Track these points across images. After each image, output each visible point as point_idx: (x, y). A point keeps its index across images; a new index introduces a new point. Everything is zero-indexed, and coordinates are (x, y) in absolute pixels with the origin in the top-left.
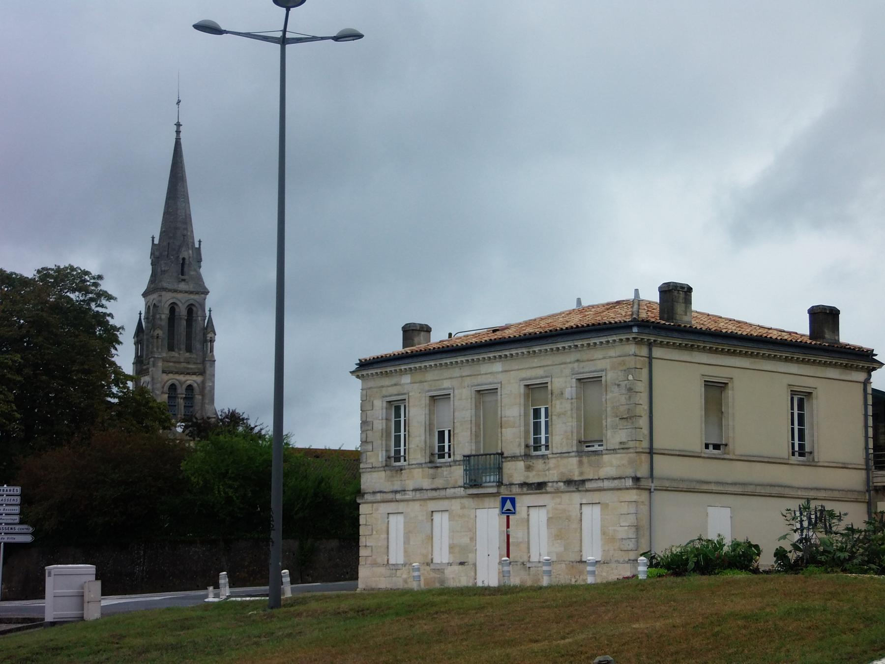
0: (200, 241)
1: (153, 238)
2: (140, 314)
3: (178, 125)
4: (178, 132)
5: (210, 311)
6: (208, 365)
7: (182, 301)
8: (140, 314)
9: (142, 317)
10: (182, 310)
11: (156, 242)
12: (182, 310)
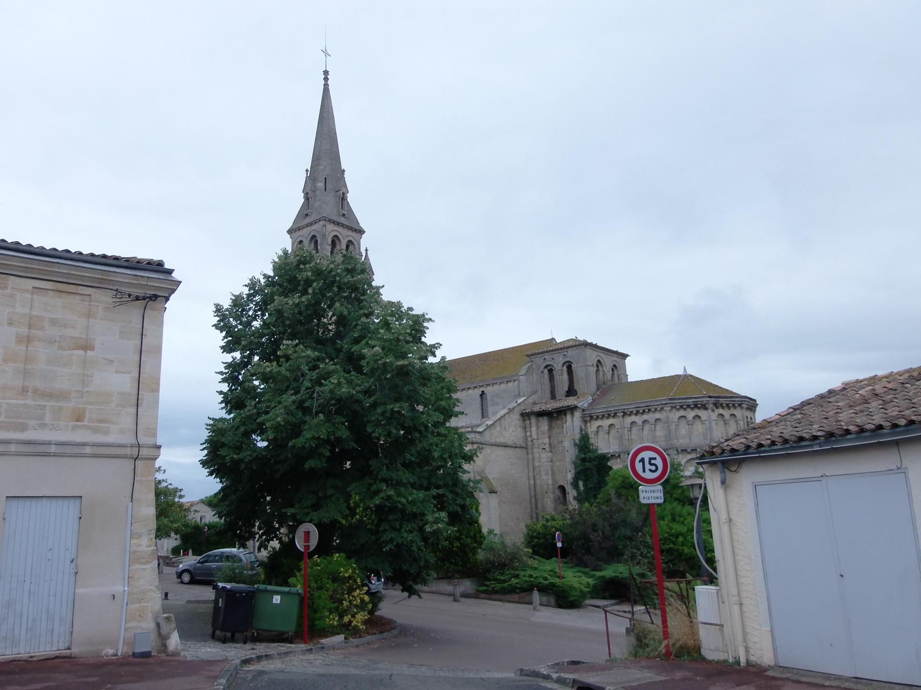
3: (326, 73)
4: (326, 79)
5: (366, 250)
12: (344, 243)
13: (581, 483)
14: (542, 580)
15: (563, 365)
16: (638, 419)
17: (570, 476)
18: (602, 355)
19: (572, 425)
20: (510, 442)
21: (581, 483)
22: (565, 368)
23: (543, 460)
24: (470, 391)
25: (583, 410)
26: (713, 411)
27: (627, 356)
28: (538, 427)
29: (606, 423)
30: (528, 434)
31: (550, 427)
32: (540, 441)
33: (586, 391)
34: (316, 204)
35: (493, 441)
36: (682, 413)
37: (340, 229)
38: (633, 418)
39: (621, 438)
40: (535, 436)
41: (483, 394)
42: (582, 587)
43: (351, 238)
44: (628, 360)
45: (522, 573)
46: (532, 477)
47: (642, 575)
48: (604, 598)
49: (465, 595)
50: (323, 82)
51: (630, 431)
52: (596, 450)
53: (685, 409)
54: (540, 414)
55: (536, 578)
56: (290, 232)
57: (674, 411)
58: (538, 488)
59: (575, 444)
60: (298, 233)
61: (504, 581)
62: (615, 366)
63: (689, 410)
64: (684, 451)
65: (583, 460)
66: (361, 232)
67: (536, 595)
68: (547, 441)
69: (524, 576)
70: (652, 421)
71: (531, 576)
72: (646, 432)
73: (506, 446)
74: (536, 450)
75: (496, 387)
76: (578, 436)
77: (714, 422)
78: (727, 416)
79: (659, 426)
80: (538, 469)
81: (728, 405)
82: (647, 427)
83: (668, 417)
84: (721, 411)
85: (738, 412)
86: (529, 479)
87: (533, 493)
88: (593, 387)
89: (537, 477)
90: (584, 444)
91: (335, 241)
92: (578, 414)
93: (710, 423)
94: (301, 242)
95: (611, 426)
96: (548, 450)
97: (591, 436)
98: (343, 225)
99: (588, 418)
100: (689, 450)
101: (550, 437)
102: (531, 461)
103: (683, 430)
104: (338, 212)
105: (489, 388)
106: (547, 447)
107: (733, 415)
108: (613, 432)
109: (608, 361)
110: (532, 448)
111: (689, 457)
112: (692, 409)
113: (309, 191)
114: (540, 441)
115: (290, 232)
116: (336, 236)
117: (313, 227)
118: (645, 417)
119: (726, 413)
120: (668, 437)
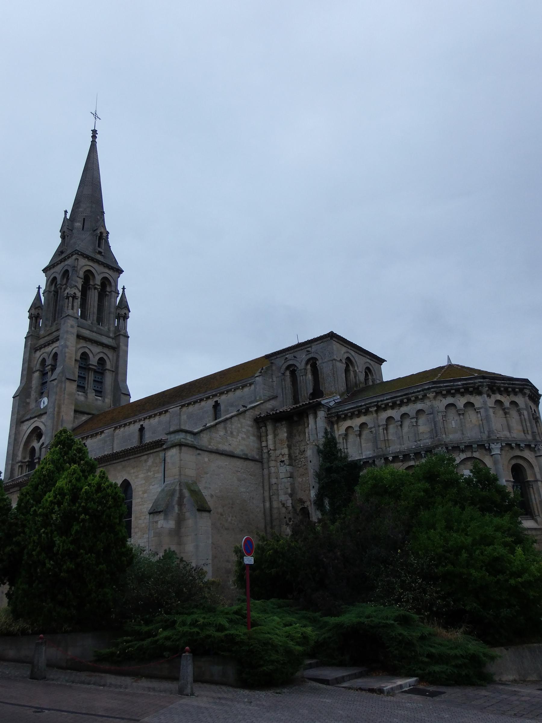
2: (39, 288)
3: (94, 132)
4: (94, 137)
5: (124, 288)
6: (122, 338)
8: (39, 288)
9: (42, 291)
12: (98, 281)
13: (326, 501)
14: (211, 631)
15: (307, 364)
16: (395, 413)
17: (313, 494)
18: (353, 353)
19: (316, 426)
20: (237, 452)
21: (326, 501)
22: (309, 367)
23: (282, 476)
24: (203, 403)
25: (329, 409)
26: (489, 396)
27: (384, 361)
28: (275, 435)
29: (356, 422)
30: (264, 444)
31: (290, 436)
32: (278, 452)
33: (333, 389)
34: (72, 241)
35: (213, 446)
36: (450, 400)
37: (95, 265)
38: (390, 413)
39: (375, 441)
40: (271, 446)
41: (216, 406)
42: (291, 644)
43: (107, 275)
44: (384, 366)
45: (179, 619)
46: (267, 499)
47: (404, 621)
48: (341, 664)
49: (75, 666)
50: (91, 139)
51: (387, 429)
52: (346, 457)
53: (453, 395)
54: (277, 418)
55: (203, 627)
56: (45, 270)
57: (440, 397)
58: (275, 511)
59: (319, 451)
60: (52, 271)
61: (149, 634)
62: (368, 368)
63: (458, 396)
64: (456, 448)
65: (329, 470)
66: (120, 271)
67: (187, 666)
68: (286, 451)
69: (184, 624)
70: (413, 413)
71: (194, 624)
72: (406, 429)
73: (231, 455)
74: (272, 464)
75: (231, 394)
76: (322, 441)
78: (507, 404)
79: (422, 420)
80: (274, 487)
81: (506, 389)
82: (407, 423)
83: (432, 407)
84: (499, 397)
85: (521, 400)
86: (264, 502)
87: (268, 518)
88: (342, 387)
89: (275, 497)
90: (329, 450)
91: (88, 276)
92: (321, 414)
93: (486, 410)
94: (55, 279)
95: (363, 425)
96: (287, 462)
97: (340, 440)
99: (335, 417)
100: (462, 447)
101: (289, 447)
102: (266, 477)
103: (453, 422)
104: (94, 249)
105: (223, 397)
106: (286, 458)
107: (513, 403)
108: (365, 432)
109: (360, 362)
110: (269, 461)
111: (463, 456)
112: (462, 394)
113: (66, 230)
114: (278, 452)
115: (45, 270)
116: (89, 271)
117: (66, 263)
118: (404, 409)
119: (506, 400)
120: (434, 432)
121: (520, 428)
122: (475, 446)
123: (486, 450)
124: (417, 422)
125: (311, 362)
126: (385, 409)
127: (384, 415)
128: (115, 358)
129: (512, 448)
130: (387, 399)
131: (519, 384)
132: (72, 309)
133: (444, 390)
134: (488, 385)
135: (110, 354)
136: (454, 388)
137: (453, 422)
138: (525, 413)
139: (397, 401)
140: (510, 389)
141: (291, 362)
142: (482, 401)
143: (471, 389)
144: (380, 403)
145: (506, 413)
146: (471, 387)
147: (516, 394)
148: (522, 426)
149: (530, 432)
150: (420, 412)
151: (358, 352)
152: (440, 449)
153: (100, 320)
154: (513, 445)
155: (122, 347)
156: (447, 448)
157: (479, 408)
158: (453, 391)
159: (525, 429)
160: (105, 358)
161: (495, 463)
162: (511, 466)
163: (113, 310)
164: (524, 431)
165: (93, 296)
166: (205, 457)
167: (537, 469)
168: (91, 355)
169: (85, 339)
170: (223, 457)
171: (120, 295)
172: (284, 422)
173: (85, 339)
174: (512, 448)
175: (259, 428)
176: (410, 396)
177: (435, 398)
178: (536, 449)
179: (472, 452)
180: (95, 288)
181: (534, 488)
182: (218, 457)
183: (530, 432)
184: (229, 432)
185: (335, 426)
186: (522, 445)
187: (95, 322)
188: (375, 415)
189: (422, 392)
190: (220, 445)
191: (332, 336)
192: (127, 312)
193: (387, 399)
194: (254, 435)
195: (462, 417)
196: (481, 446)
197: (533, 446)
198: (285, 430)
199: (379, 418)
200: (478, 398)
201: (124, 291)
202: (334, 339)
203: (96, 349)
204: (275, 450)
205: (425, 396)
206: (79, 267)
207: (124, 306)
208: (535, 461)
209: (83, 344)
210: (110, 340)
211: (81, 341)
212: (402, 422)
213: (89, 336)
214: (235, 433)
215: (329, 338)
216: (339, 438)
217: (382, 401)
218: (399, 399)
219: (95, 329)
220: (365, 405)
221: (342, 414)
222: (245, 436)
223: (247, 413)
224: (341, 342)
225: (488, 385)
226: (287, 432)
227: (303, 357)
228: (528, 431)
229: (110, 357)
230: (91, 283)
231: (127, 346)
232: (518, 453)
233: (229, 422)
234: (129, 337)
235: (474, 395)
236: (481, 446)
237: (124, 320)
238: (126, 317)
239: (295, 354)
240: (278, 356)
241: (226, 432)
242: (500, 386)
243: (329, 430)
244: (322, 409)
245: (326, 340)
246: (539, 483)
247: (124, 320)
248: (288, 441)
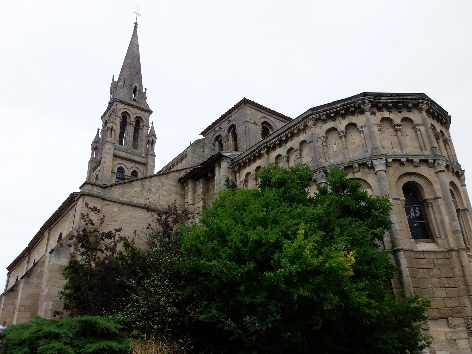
0: (146, 89)
1: (113, 76)
2: (98, 130)
3: (136, 24)
4: (136, 27)
5: (153, 123)
6: (150, 157)
7: (133, 113)
8: (98, 130)
9: (100, 131)
10: (132, 118)
11: (116, 79)
12: (132, 118)
15: (229, 132)
18: (272, 119)
22: (231, 134)
28: (194, 192)
30: (186, 201)
35: (125, 199)
43: (139, 115)
53: (334, 119)
57: (320, 124)
63: (339, 119)
66: (150, 112)
70: (296, 146)
77: (376, 129)
79: (306, 151)
84: (386, 114)
91: (125, 116)
93: (369, 128)
98: (132, 106)
101: (204, 200)
103: (335, 144)
107: (405, 120)
112: (343, 116)
114: (196, 206)
118: (290, 144)
119: (396, 117)
121: (417, 145)
122: (356, 165)
123: (369, 168)
124: (301, 154)
125: (232, 129)
126: (274, 148)
127: (273, 155)
128: (145, 171)
129: (402, 164)
130: (274, 138)
131: (411, 99)
132: (111, 137)
133: (322, 115)
134: (371, 102)
135: (141, 168)
136: (334, 110)
137: (335, 147)
138: (423, 129)
139: (282, 137)
140: (400, 105)
141: (218, 134)
142: (365, 119)
143: (352, 109)
144: (269, 144)
145: (396, 131)
146: (352, 107)
147: (409, 110)
148: (419, 142)
149: (428, 148)
150: (303, 143)
151: (279, 118)
152: (318, 173)
153: (135, 146)
154: (404, 160)
155: (150, 162)
156: (325, 172)
157: (362, 127)
158: (332, 115)
159: (423, 145)
160: (137, 171)
161: (379, 180)
162: (401, 185)
163: (144, 138)
164: (421, 147)
165: (130, 130)
166: (116, 208)
167: (437, 186)
168: (125, 169)
169: (120, 158)
170: (137, 209)
171: (150, 128)
172: (201, 180)
173: (120, 158)
174: (402, 164)
175: (183, 188)
176: (293, 128)
177: (314, 125)
178: (436, 164)
179: (354, 173)
180: (131, 124)
181: (435, 207)
182: (132, 209)
183: (428, 148)
184: (147, 189)
185: (237, 175)
186: (415, 160)
187: (131, 147)
188: (266, 156)
189: (302, 123)
190: (134, 199)
191: (245, 102)
192: (154, 139)
193: (274, 138)
194: (177, 193)
195: (343, 139)
196: (363, 165)
197: (431, 161)
198: (201, 186)
199: (270, 158)
200: (361, 117)
201: (153, 125)
202: (248, 105)
203: (129, 165)
204: (194, 204)
205: (306, 126)
206: (118, 110)
207: (153, 134)
208: (435, 178)
209: (119, 161)
210: (142, 159)
211: (118, 159)
212: (288, 157)
213: (124, 156)
214: (154, 190)
215: (243, 105)
216: (240, 185)
217: (270, 141)
218: (283, 134)
219: (130, 151)
220: (257, 148)
221: (241, 162)
222: (165, 193)
223: (170, 174)
224: (257, 109)
225: (371, 102)
226: (203, 187)
227: (226, 126)
228: (425, 147)
229: (142, 170)
230: (128, 120)
231: (154, 162)
232: (410, 169)
233: (147, 181)
234: (155, 156)
235: (357, 115)
236: (363, 165)
237: (152, 144)
238: (153, 142)
239: (221, 126)
240: (210, 131)
241: (143, 188)
242: (386, 102)
243: (231, 178)
244: (225, 160)
245: (241, 107)
246: (440, 201)
247: (152, 144)
248: (204, 195)
